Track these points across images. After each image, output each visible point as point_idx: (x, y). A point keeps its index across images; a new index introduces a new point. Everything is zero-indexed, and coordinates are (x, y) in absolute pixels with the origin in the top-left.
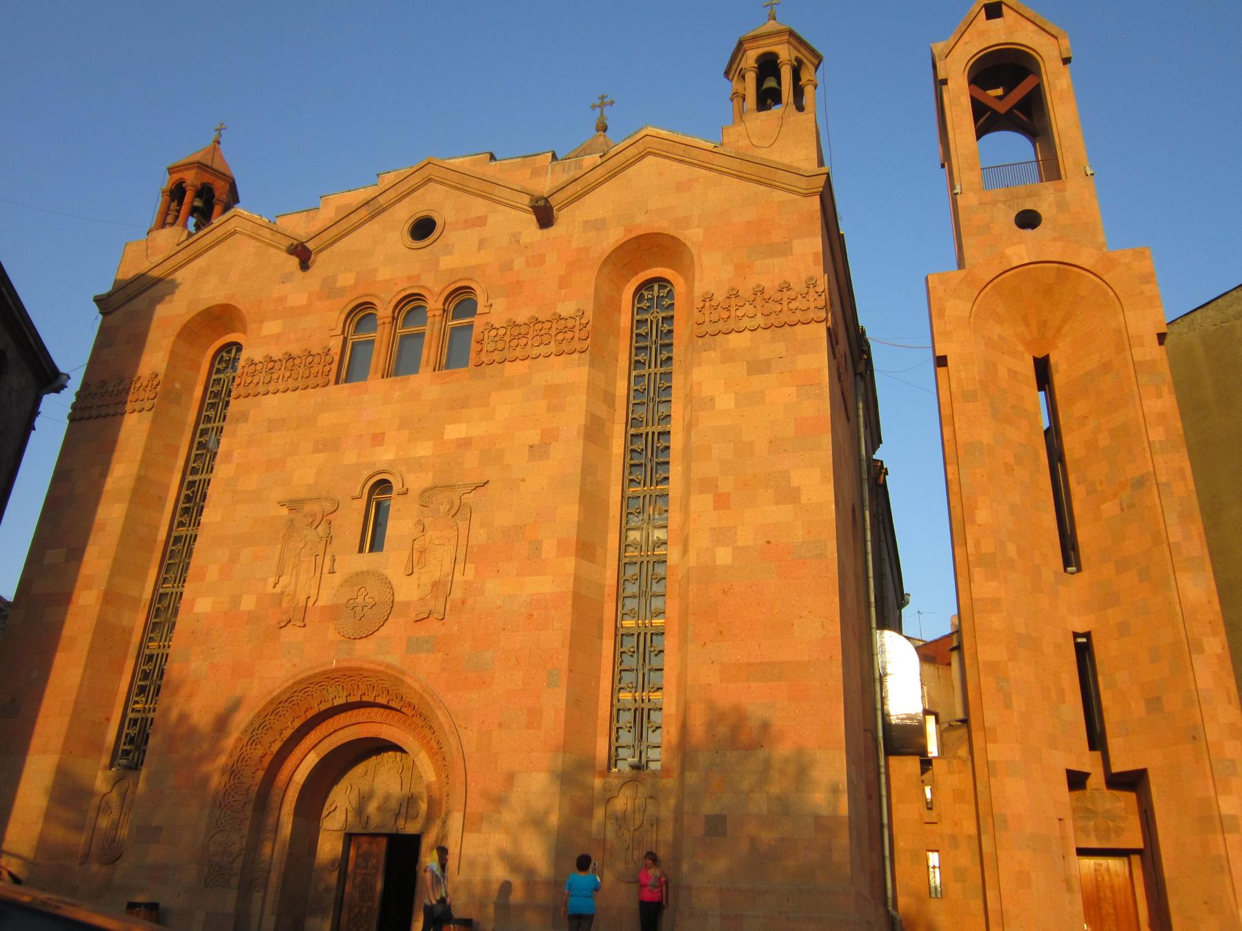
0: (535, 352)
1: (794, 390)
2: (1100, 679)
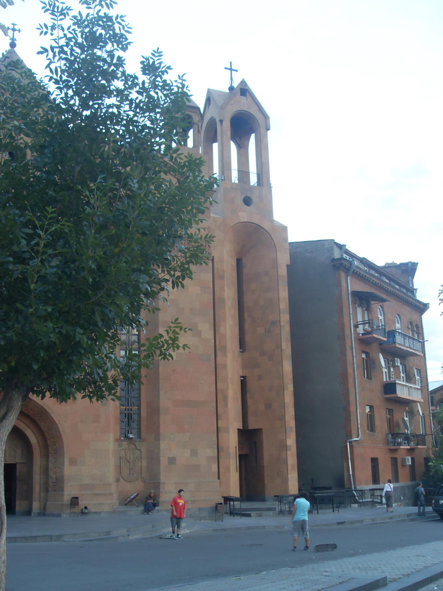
2: (248, 394)
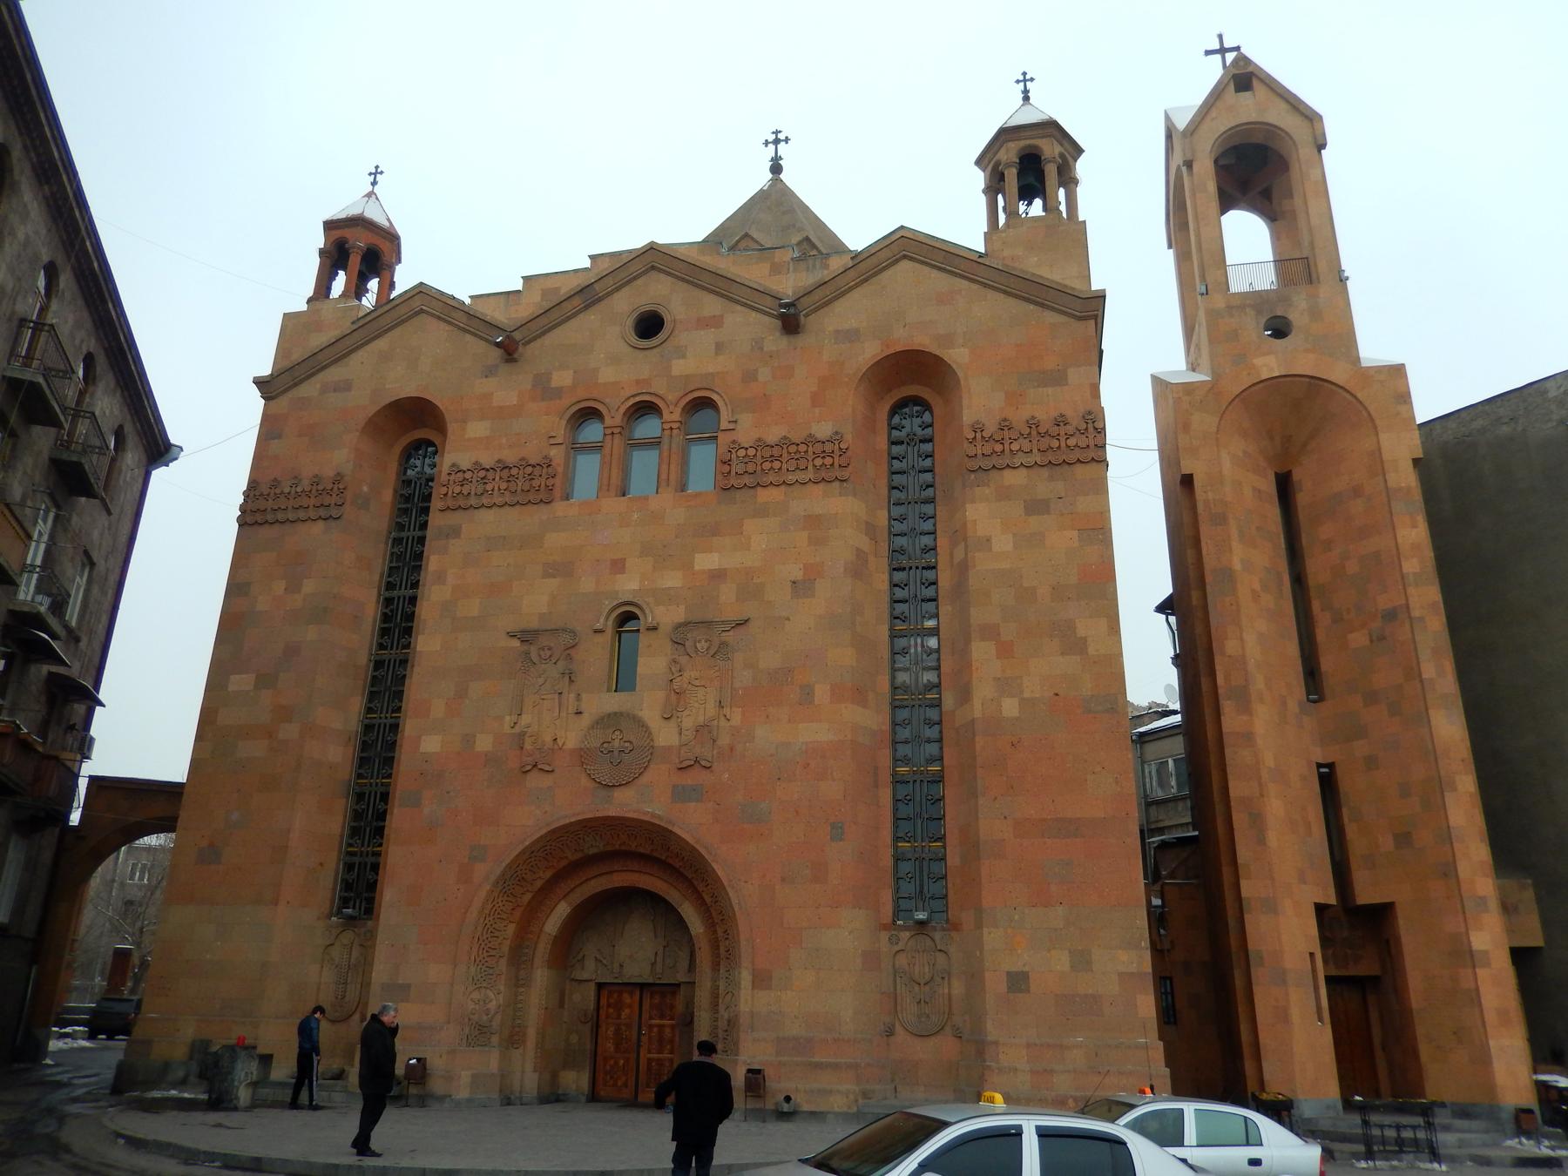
0: (791, 478)
1: (1076, 533)
2: (1345, 811)
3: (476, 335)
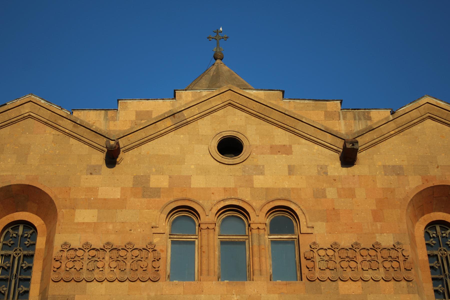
0: (367, 275)
3: (80, 140)
